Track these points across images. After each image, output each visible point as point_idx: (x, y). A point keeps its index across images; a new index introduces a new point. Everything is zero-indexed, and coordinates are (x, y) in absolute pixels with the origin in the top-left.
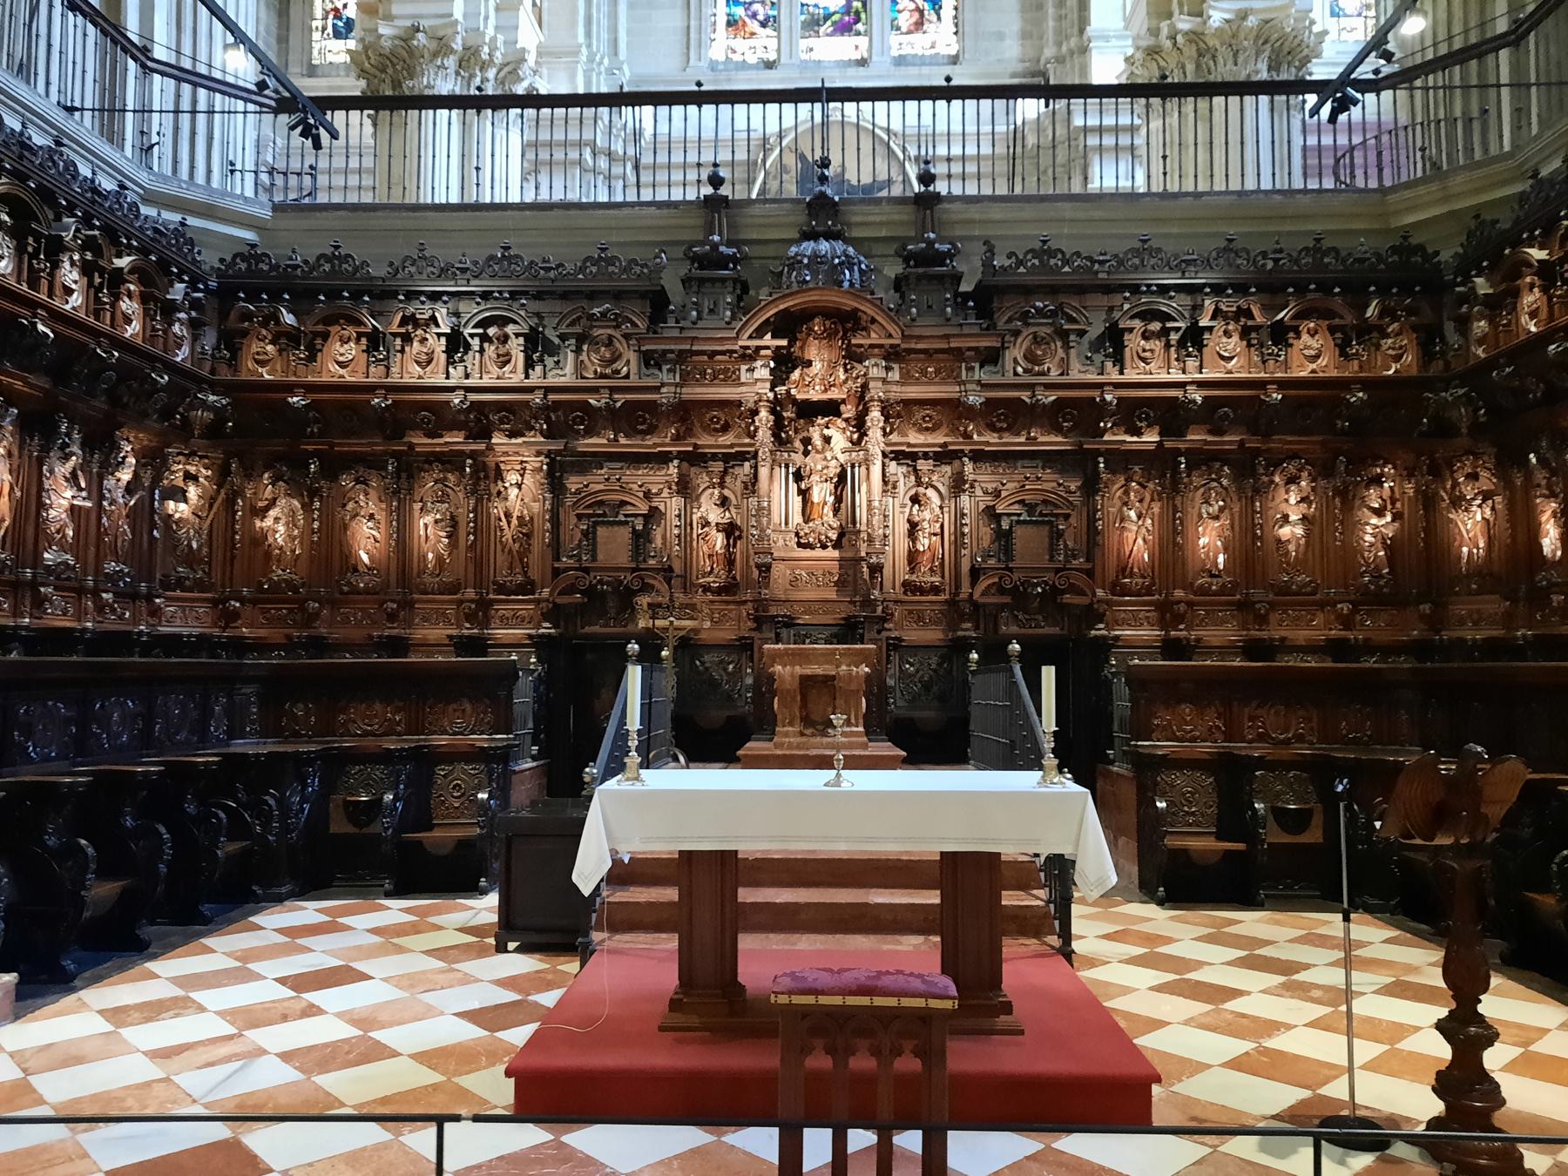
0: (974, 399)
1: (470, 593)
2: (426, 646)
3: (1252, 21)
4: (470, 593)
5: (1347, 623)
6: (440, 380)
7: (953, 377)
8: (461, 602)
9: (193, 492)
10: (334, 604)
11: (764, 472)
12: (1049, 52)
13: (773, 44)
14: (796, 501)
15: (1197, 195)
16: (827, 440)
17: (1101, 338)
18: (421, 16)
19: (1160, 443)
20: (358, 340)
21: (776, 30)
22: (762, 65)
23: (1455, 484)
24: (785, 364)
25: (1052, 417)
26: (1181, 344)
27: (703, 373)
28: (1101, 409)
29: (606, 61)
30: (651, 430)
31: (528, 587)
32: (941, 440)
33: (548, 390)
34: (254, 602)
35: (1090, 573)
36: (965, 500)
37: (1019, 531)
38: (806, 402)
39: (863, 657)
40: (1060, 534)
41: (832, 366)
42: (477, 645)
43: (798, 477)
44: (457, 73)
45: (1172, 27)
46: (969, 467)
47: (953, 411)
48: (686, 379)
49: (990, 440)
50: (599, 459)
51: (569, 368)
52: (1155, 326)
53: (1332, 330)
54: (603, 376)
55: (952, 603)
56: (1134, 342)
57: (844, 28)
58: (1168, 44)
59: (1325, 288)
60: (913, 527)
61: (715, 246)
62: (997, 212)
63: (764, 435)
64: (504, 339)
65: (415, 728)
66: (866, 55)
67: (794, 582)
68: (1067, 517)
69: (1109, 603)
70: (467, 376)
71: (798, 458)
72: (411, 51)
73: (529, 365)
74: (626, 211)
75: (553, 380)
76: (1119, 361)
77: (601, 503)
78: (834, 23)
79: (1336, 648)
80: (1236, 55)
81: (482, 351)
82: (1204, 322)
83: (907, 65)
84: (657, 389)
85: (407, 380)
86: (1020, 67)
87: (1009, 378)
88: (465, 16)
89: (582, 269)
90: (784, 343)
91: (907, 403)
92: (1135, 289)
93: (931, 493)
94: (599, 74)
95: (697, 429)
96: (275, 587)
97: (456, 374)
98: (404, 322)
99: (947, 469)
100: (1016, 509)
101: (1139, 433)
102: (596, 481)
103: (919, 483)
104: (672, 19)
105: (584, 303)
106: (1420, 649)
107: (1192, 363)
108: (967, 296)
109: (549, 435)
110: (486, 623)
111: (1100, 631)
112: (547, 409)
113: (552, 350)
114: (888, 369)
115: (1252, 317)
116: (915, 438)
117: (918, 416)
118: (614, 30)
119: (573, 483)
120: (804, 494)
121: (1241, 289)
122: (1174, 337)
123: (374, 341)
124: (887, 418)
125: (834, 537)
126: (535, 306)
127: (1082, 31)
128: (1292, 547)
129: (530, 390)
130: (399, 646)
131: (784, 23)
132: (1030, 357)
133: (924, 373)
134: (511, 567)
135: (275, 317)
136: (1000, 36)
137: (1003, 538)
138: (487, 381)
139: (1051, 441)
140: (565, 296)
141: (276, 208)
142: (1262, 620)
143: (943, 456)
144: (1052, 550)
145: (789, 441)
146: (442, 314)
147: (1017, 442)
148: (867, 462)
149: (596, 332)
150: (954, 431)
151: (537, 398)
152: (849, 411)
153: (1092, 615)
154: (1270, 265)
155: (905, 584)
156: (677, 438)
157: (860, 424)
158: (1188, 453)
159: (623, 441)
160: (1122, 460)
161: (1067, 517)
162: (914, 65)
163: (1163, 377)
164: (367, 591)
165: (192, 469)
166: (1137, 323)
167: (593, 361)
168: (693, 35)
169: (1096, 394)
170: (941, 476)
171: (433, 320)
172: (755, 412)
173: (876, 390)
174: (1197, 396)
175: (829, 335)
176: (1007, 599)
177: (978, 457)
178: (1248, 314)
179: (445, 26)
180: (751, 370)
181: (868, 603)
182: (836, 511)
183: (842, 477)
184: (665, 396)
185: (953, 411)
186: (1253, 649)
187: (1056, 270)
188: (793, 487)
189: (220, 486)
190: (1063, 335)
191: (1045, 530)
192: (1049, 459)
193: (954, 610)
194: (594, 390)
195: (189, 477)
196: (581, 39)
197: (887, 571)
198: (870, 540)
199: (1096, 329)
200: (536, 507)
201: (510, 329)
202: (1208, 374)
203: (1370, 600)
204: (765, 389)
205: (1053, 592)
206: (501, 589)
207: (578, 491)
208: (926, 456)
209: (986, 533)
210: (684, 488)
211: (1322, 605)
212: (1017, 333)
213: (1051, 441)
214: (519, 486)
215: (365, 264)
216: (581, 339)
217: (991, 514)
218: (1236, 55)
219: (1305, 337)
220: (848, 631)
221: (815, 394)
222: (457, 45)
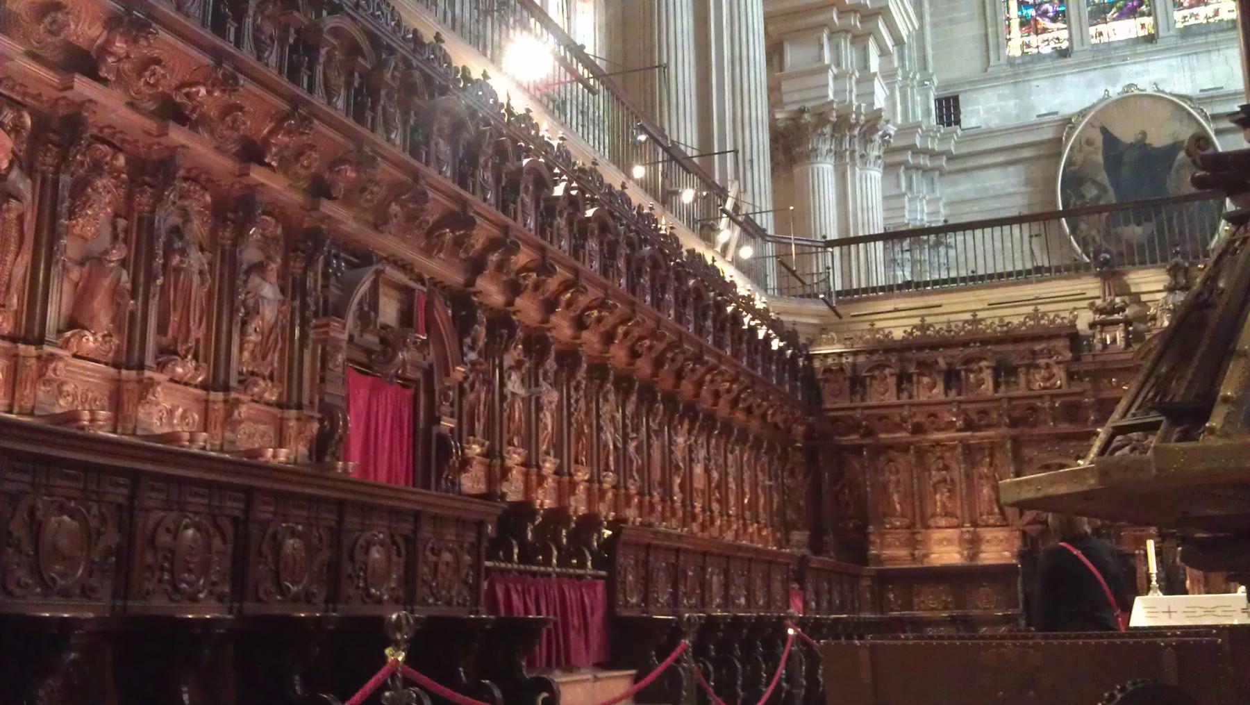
13: (1064, 34)
18: (804, 101)
22: (1056, 55)
29: (918, 77)
33: (1010, 399)
44: (832, 136)
64: (981, 370)
66: (1153, 32)
73: (997, 386)
78: (1120, 9)
88: (835, 93)
94: (912, 88)
104: (969, 31)
162: (1201, 34)
168: (991, 40)
179: (823, 105)
196: (896, 64)
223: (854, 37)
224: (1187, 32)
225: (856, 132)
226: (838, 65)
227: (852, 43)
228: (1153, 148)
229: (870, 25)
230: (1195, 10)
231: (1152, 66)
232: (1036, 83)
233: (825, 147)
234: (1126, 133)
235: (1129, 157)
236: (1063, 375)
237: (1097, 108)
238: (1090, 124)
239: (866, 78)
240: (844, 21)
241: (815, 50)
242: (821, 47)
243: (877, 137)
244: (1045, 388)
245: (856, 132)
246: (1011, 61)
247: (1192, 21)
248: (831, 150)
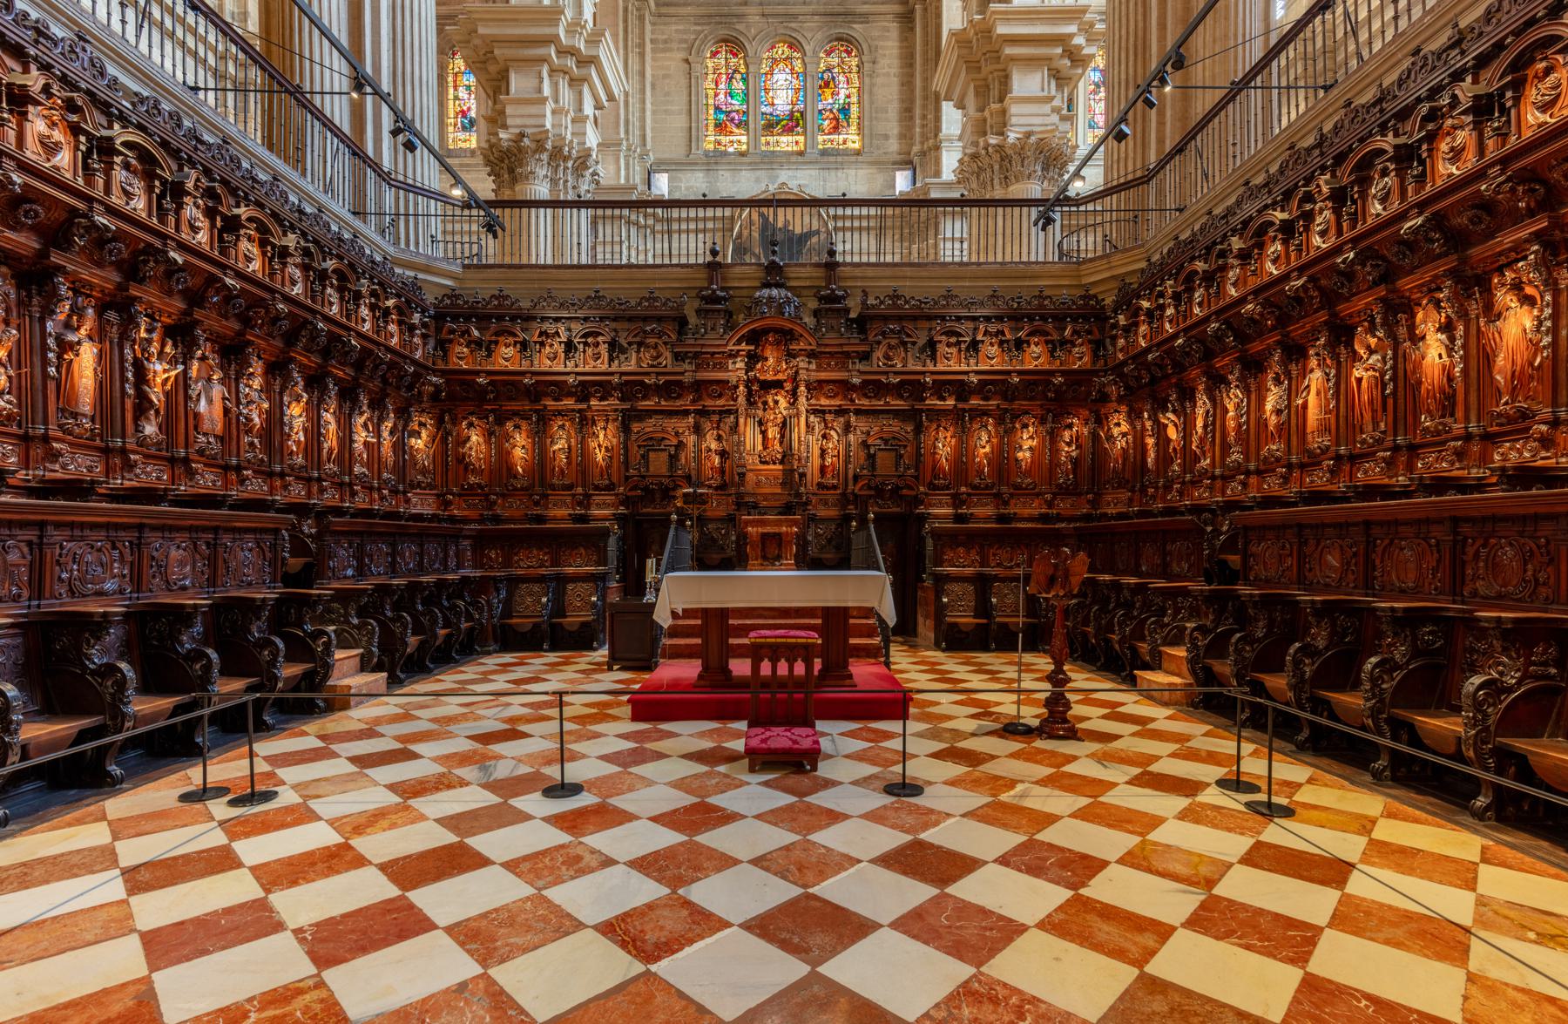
0: (856, 381)
1: (580, 490)
2: (555, 519)
3: (1033, 139)
4: (580, 490)
5: (1050, 505)
6: (561, 368)
7: (844, 368)
8: (574, 495)
9: (424, 434)
10: (504, 496)
11: (742, 421)
12: (916, 149)
14: (759, 438)
15: (979, 264)
16: (776, 402)
17: (924, 346)
18: (526, 126)
19: (955, 406)
20: (515, 346)
21: (747, 130)
23: (1109, 429)
24: (753, 359)
25: (897, 390)
26: (967, 349)
27: (708, 365)
28: (923, 386)
30: (679, 397)
31: (610, 487)
32: (838, 403)
34: (460, 495)
35: (916, 478)
36: (851, 437)
37: (879, 454)
38: (765, 381)
39: (795, 523)
40: (901, 456)
41: (779, 361)
42: (583, 519)
43: (760, 423)
44: (549, 164)
45: (986, 141)
46: (853, 419)
47: (844, 387)
48: (698, 367)
49: (864, 403)
50: (650, 413)
51: (633, 362)
52: (953, 340)
53: (1047, 342)
54: (652, 366)
55: (844, 494)
56: (942, 349)
57: (789, 130)
58: (983, 152)
59: (1043, 318)
60: (823, 452)
61: (714, 291)
62: (870, 272)
63: (742, 400)
64: (597, 345)
65: (555, 563)
67: (758, 483)
68: (905, 446)
69: (926, 494)
70: (576, 366)
71: (760, 413)
72: (520, 150)
73: (611, 360)
74: (663, 270)
75: (624, 369)
76: (934, 358)
77: (651, 439)
79: (1044, 518)
80: (1023, 161)
81: (584, 352)
82: (979, 338)
83: (829, 155)
84: (682, 374)
85: (543, 369)
87: (875, 368)
88: (553, 126)
89: (640, 304)
90: (752, 348)
91: (820, 382)
92: (943, 318)
93: (833, 433)
95: (705, 396)
96: (471, 487)
97: (570, 364)
98: (541, 334)
99: (842, 419)
100: (878, 442)
101: (944, 399)
102: (649, 425)
103: (826, 427)
104: (680, 122)
105: (641, 324)
106: (1087, 518)
107: (972, 361)
108: (852, 321)
109: (622, 400)
110: (588, 507)
111: (921, 510)
112: (620, 386)
113: (623, 351)
114: (809, 363)
115: (1004, 335)
116: (824, 401)
117: (826, 388)
118: (643, 128)
119: (636, 427)
120: (764, 433)
121: (1000, 319)
122: (963, 346)
123: (524, 345)
124: (809, 390)
125: (779, 456)
126: (613, 325)
127: (936, 136)
128: (1023, 464)
129: (612, 374)
130: (540, 519)
131: (752, 126)
132: (887, 357)
133: (829, 365)
134: (602, 475)
135: (468, 332)
136: (886, 137)
137: (871, 458)
138: (587, 369)
139: (897, 403)
140: (630, 319)
141: (464, 267)
142: (1006, 503)
143: (840, 412)
144: (897, 465)
145: (755, 403)
146: (562, 330)
147: (879, 404)
148: (798, 415)
149: (648, 341)
150: (845, 397)
151: (616, 379)
152: (788, 386)
153: (917, 501)
154: (1015, 305)
155: (819, 484)
156: (694, 401)
157: (794, 393)
158: (971, 410)
159: (663, 403)
160: (937, 415)
161: (905, 446)
163: (957, 368)
164: (522, 489)
165: (423, 420)
166: (944, 338)
167: (647, 356)
169: (921, 377)
170: (838, 424)
171: (557, 333)
172: (737, 387)
173: (803, 375)
174: (974, 379)
175: (778, 343)
176: (873, 493)
177: (858, 412)
178: (1003, 333)
179: (541, 132)
180: (734, 363)
181: (798, 495)
182: (781, 443)
183: (784, 423)
184: (687, 378)
185: (844, 387)
186: (1001, 519)
187: (900, 307)
188: (757, 429)
189: (438, 429)
190: (904, 344)
191: (894, 454)
192: (896, 414)
193: (845, 499)
194: (647, 374)
195: (422, 424)
196: (622, 136)
197: (809, 477)
198: (799, 460)
199: (922, 341)
200: (615, 441)
201: (600, 339)
202: (981, 367)
203: (1064, 491)
204: (742, 374)
205: (897, 489)
206: (597, 488)
207: (638, 432)
208: (830, 412)
209: (862, 455)
210: (697, 430)
211: (1038, 495)
212: (879, 343)
213: (897, 403)
214: (605, 429)
215: (517, 300)
216: (640, 344)
217: (865, 445)
218: (1023, 161)
219: (1033, 346)
220: (787, 509)
221: (769, 377)
222: (549, 145)
223: (571, 80)
224: (824, 153)
225: (570, 164)
226: (556, 101)
227: (570, 85)
229: (584, 71)
230: (832, 137)
231: (799, 174)
232: (721, 173)
233: (542, 172)
236: (668, 354)
239: (579, 119)
240: (562, 61)
241: (534, 82)
242: (541, 81)
243: (588, 173)
244: (652, 366)
245: (570, 164)
246: (706, 153)
247: (829, 145)
248: (546, 176)
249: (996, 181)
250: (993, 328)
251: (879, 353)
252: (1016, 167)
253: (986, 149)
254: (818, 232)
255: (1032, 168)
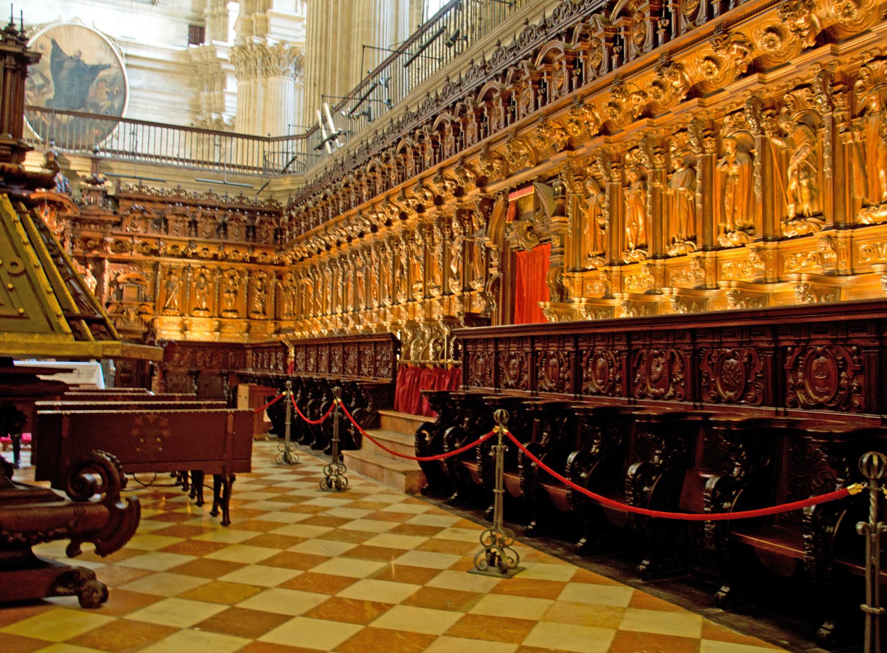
45: (251, 40)
76: (167, 231)
80: (279, 61)
86: (191, 14)
87: (124, 232)
187: (145, 194)
218: (279, 61)
228: (85, 65)
234: (69, 49)
235: (67, 64)
237: (52, 26)
238: (45, 35)
249: (259, 71)
250: (209, 211)
251: (126, 222)
252: (274, 65)
253: (251, 45)
254: (109, 66)
255: (286, 68)
